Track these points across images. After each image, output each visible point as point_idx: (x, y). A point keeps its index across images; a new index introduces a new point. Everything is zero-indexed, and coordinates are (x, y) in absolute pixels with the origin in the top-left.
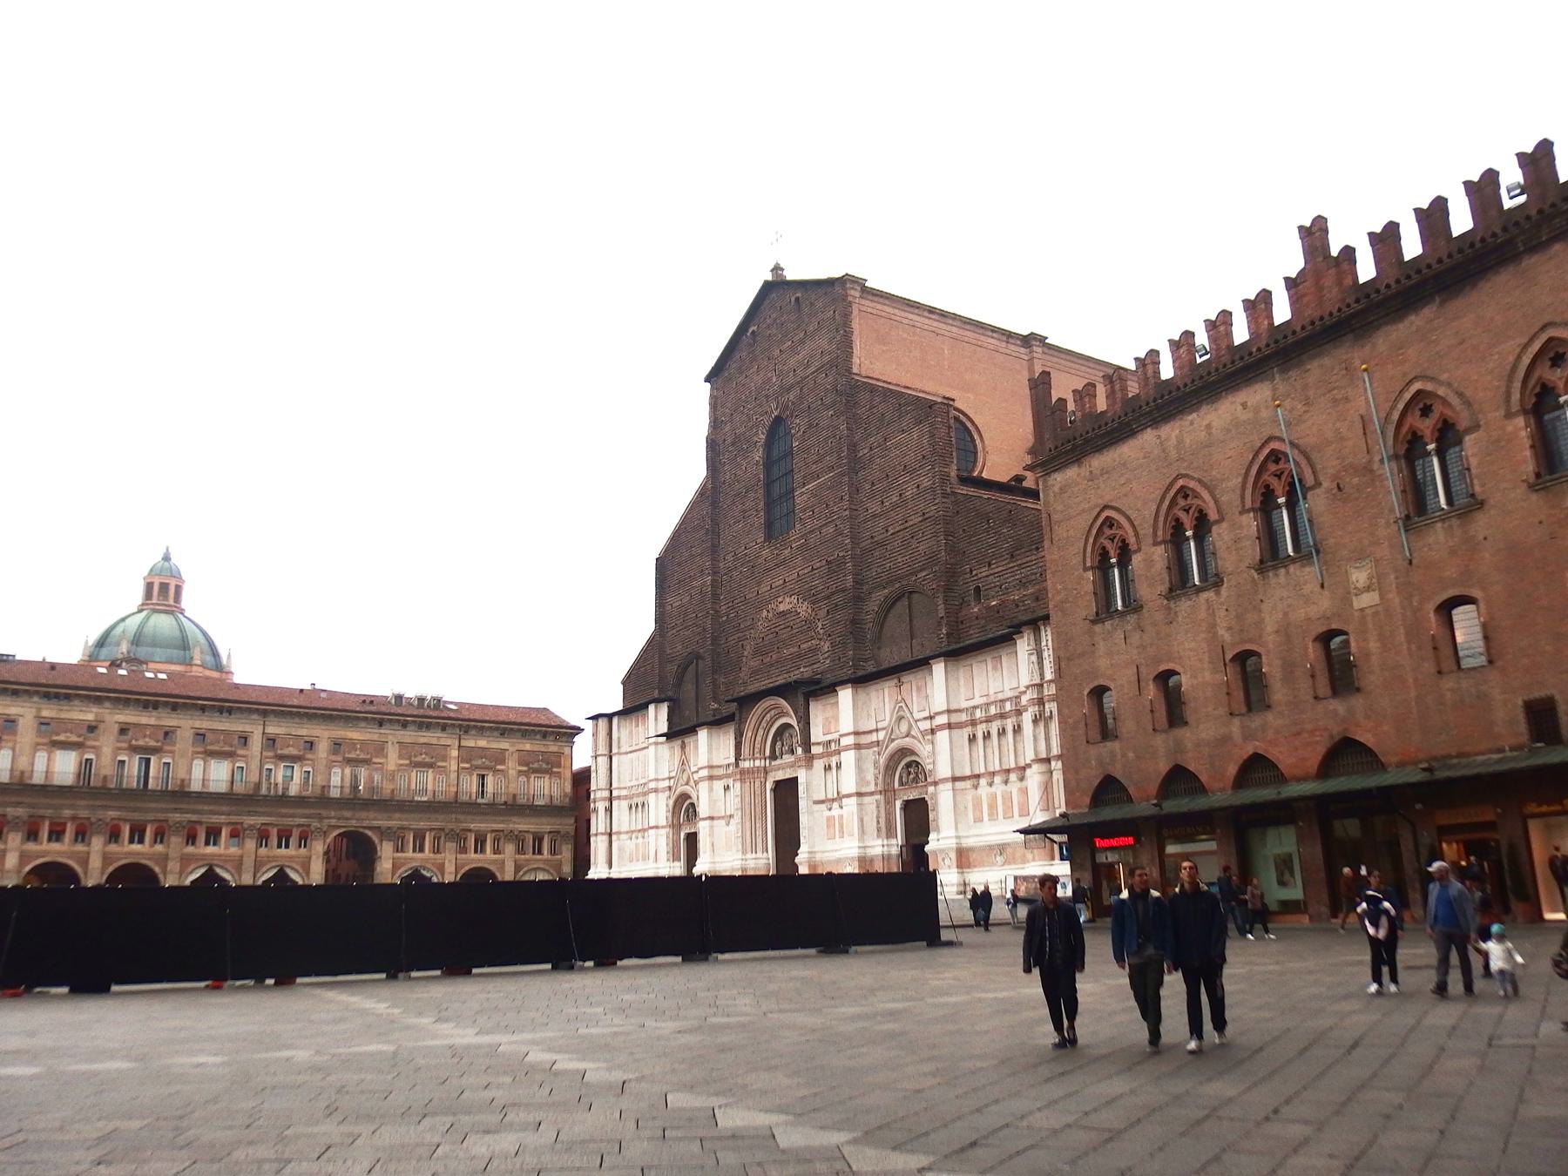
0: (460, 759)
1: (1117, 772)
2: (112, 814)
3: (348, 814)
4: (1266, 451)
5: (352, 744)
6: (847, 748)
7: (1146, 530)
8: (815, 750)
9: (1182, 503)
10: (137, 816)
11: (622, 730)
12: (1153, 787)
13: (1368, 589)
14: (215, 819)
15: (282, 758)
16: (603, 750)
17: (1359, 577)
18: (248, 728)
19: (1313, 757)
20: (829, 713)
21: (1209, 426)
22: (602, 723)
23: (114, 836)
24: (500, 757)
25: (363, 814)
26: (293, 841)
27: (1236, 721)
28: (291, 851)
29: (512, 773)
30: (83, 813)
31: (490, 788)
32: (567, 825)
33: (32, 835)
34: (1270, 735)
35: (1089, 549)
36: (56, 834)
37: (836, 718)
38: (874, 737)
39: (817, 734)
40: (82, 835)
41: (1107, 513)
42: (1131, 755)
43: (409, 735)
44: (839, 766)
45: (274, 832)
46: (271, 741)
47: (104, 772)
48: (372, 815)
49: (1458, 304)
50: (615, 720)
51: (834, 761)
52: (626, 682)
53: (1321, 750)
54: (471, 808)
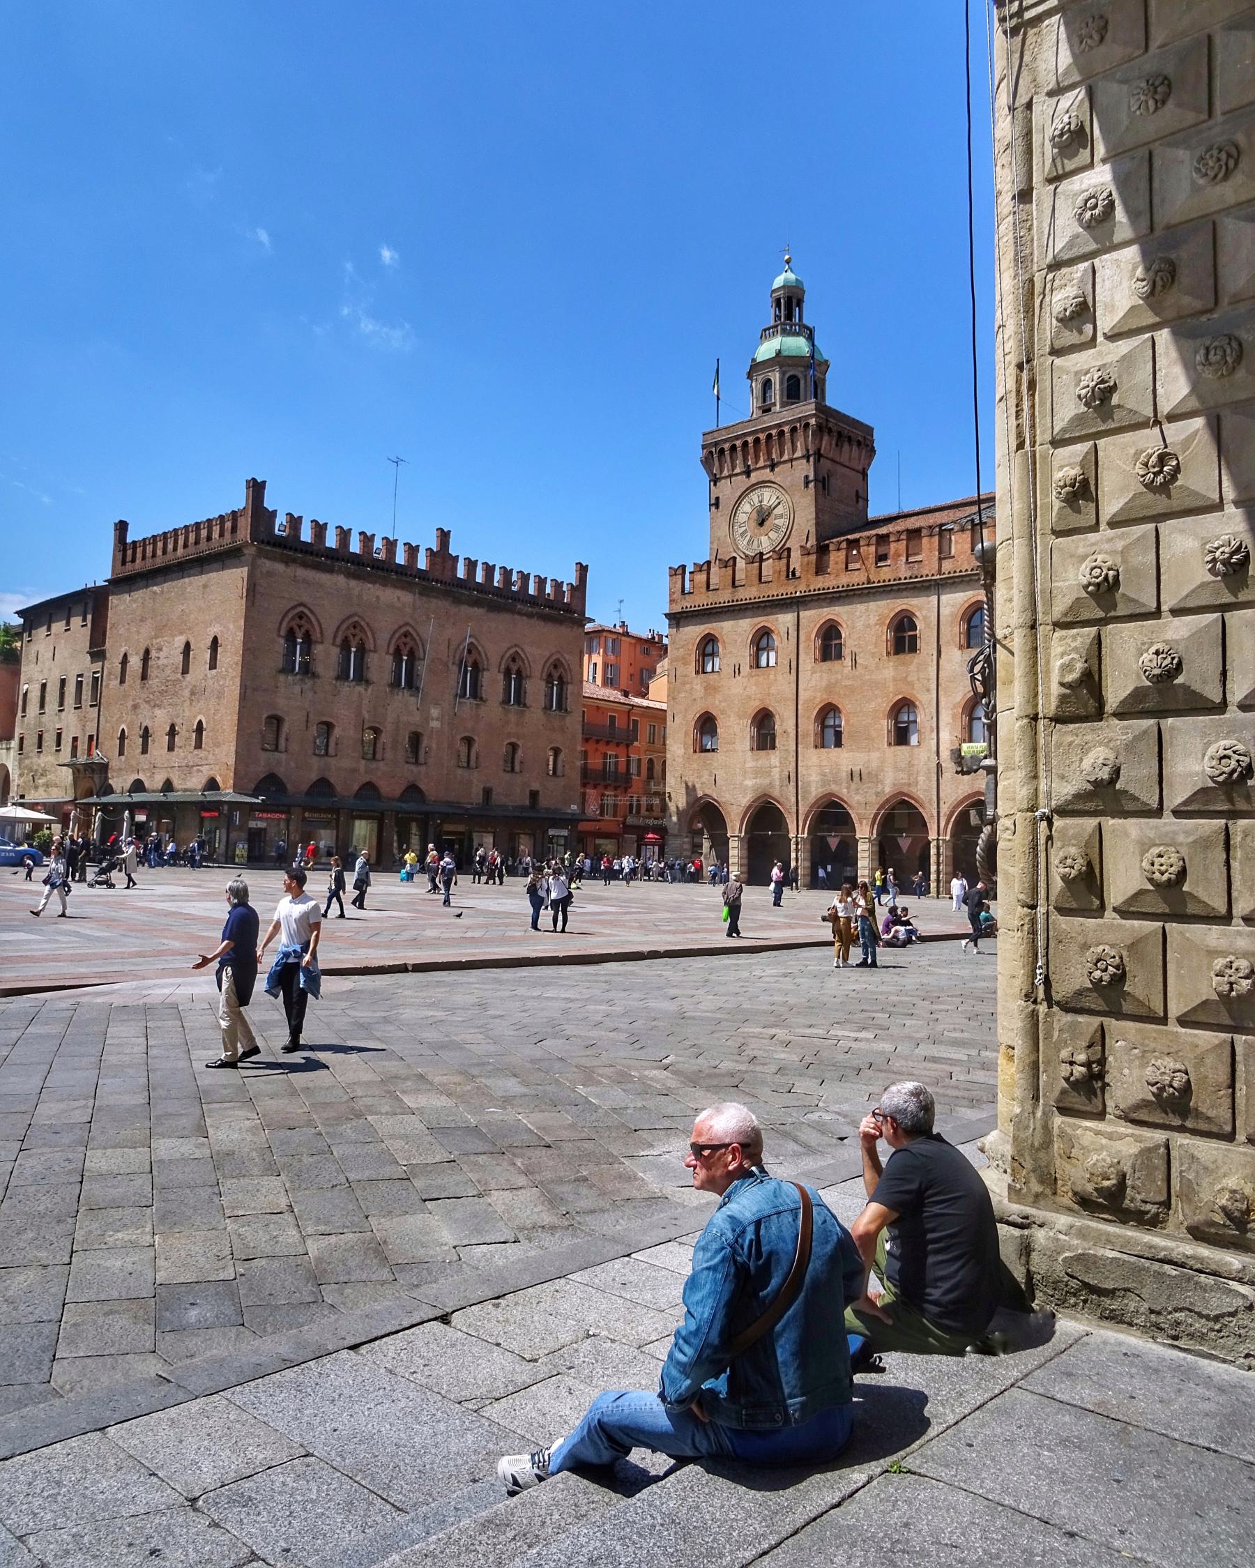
1: (281, 772)
4: (404, 629)
7: (329, 633)
9: (352, 630)
12: (305, 787)
13: (437, 719)
17: (435, 712)
19: (398, 792)
21: (378, 597)
27: (363, 762)
34: (379, 774)
35: (284, 625)
41: (301, 609)
42: (293, 765)
49: (492, 615)
53: (403, 787)
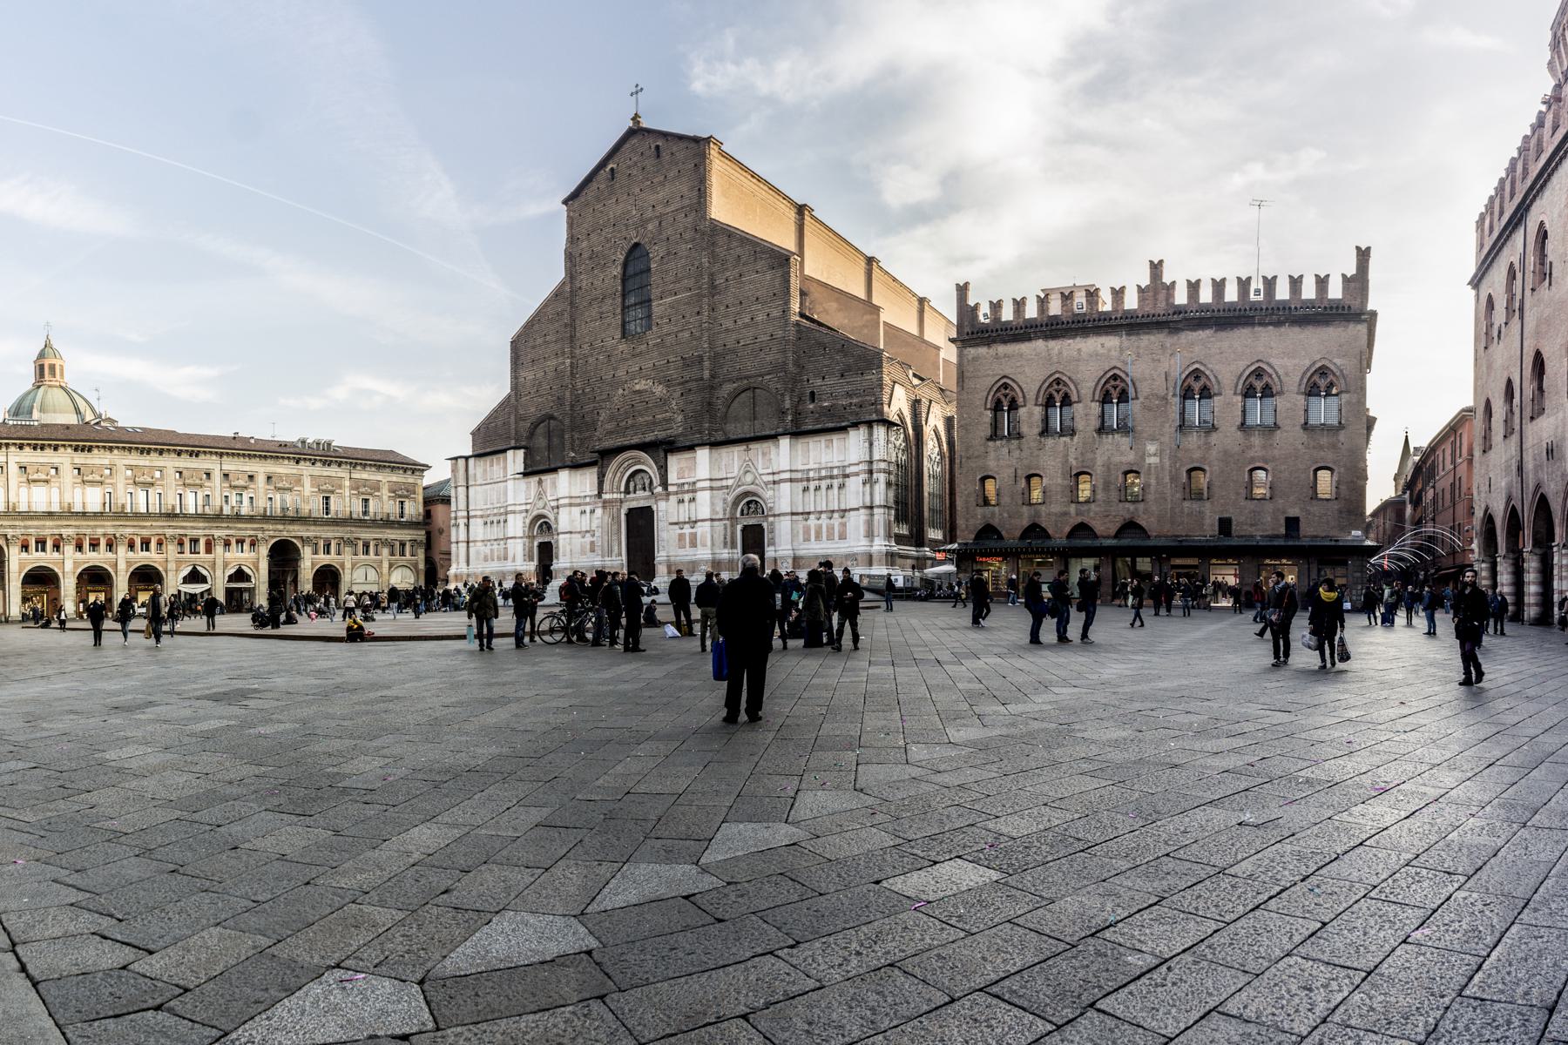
0: (352, 488)
2: (131, 530)
3: (280, 527)
5: (280, 477)
6: (703, 489)
8: (671, 489)
10: (145, 532)
11: (477, 467)
14: (195, 533)
15: (235, 487)
16: (462, 482)
18: (210, 466)
20: (684, 464)
22: (461, 462)
23: (131, 546)
24: (376, 487)
25: (291, 527)
26: (246, 546)
28: (246, 555)
29: (385, 498)
30: (110, 531)
31: (371, 509)
32: (420, 535)
33: (79, 547)
36: (94, 545)
37: (693, 468)
38: (724, 483)
39: (673, 477)
40: (110, 546)
43: (318, 470)
44: (693, 500)
45: (233, 541)
46: (226, 475)
47: (120, 502)
48: (296, 527)
50: (471, 461)
51: (687, 497)
52: (473, 434)
54: (360, 523)
